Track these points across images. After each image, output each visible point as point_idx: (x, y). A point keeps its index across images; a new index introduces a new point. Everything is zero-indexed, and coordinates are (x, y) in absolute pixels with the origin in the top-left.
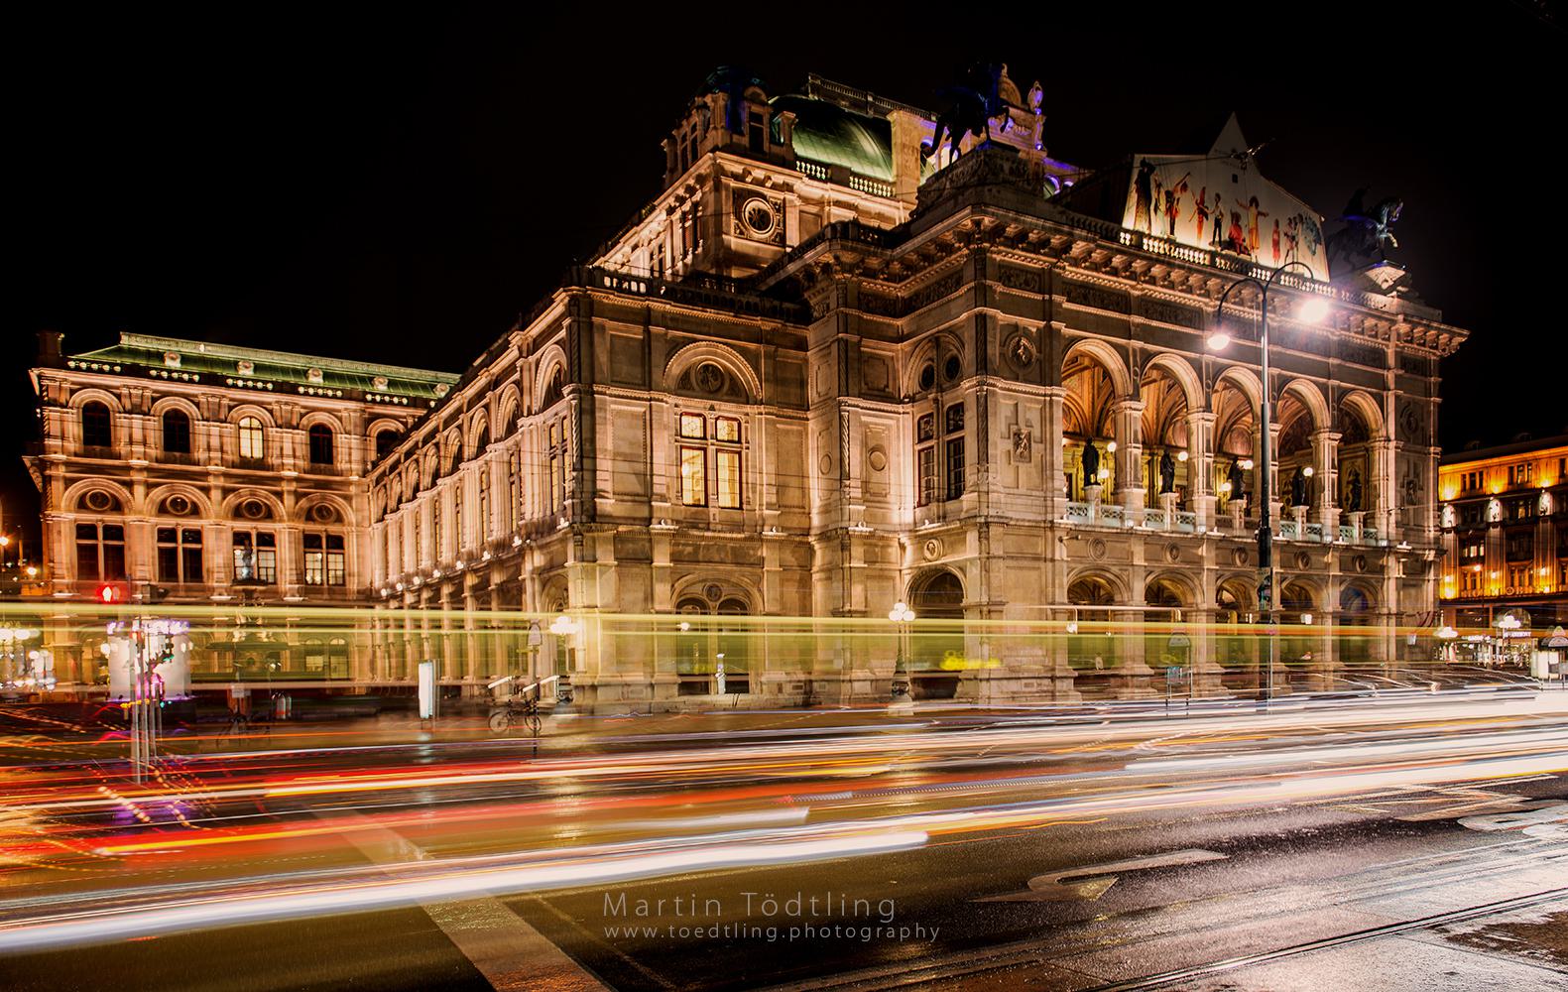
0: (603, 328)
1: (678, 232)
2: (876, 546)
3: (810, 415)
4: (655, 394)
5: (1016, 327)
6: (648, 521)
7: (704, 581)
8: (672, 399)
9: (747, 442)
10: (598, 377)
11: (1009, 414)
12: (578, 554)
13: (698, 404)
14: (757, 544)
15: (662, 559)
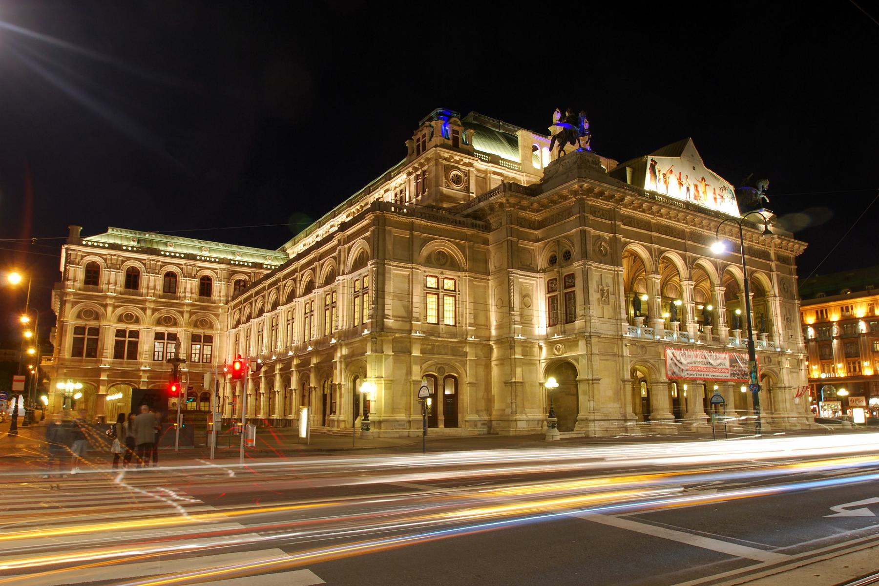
0: (390, 232)
1: (413, 184)
2: (527, 347)
3: (490, 277)
4: (415, 266)
5: (599, 237)
6: (410, 331)
7: (437, 364)
8: (423, 268)
9: (459, 291)
10: (387, 256)
11: (598, 280)
12: (374, 348)
13: (436, 271)
14: (463, 345)
15: (416, 353)
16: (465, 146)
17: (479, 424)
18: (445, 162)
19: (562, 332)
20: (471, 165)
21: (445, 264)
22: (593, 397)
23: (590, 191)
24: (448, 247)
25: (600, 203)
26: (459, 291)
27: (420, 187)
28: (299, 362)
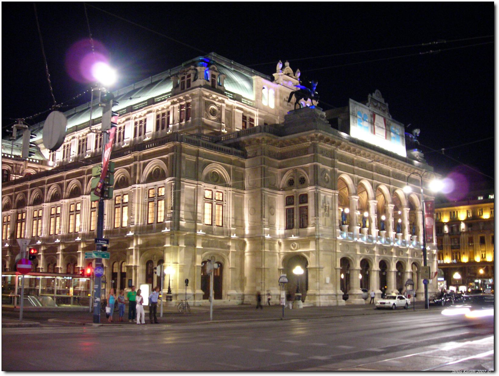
0: (184, 157)
1: (177, 111)
3: (245, 192)
4: (199, 182)
8: (204, 184)
9: (225, 201)
10: (182, 175)
12: (172, 242)
13: (211, 186)
15: (199, 246)
16: (219, 87)
17: (237, 298)
18: (206, 99)
19: (297, 234)
20: (223, 102)
21: (217, 181)
22: (319, 280)
23: (321, 138)
24: (219, 169)
26: (225, 201)
27: (184, 115)
28: (85, 246)
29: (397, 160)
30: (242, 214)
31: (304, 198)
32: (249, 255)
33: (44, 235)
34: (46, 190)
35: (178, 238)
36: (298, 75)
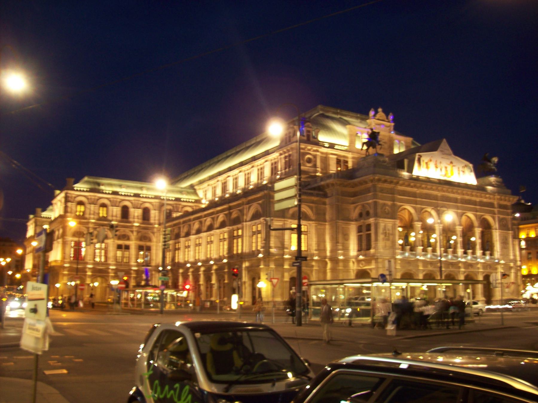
1: (283, 161)
3: (327, 223)
4: (286, 219)
8: (290, 220)
9: (309, 231)
15: (286, 267)
20: (317, 151)
23: (379, 180)
25: (386, 186)
29: (462, 189)
30: (324, 242)
31: (368, 228)
32: (330, 272)
33: (192, 260)
34: (192, 225)
35: (269, 261)
36: (391, 117)
